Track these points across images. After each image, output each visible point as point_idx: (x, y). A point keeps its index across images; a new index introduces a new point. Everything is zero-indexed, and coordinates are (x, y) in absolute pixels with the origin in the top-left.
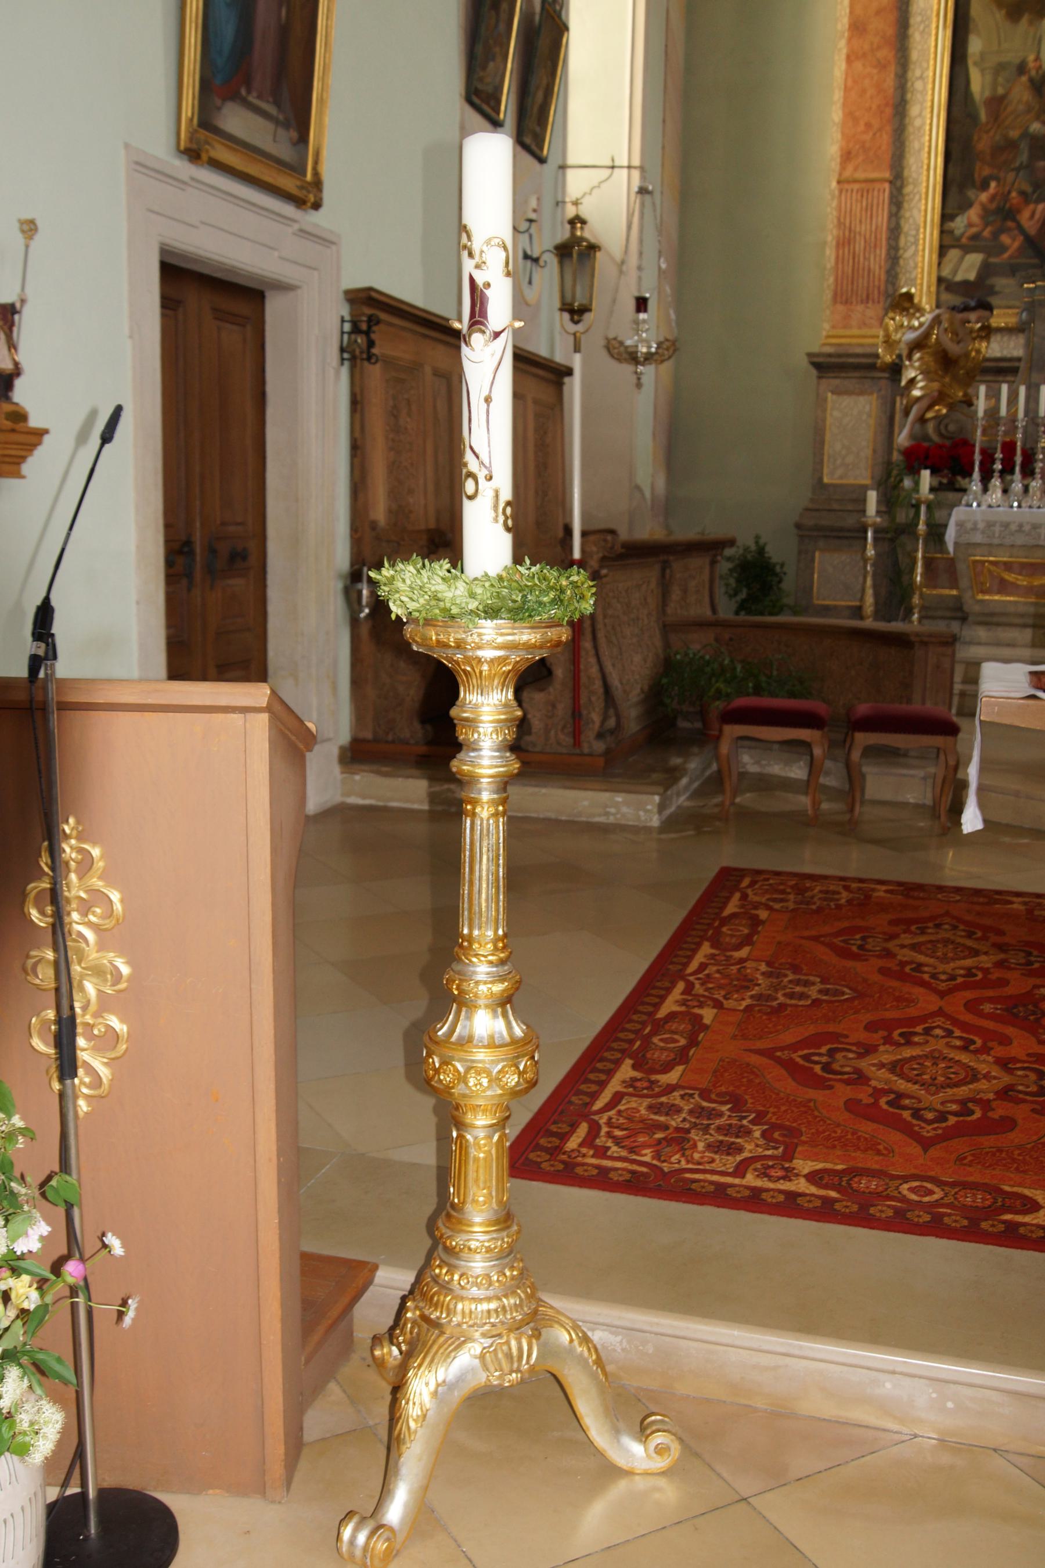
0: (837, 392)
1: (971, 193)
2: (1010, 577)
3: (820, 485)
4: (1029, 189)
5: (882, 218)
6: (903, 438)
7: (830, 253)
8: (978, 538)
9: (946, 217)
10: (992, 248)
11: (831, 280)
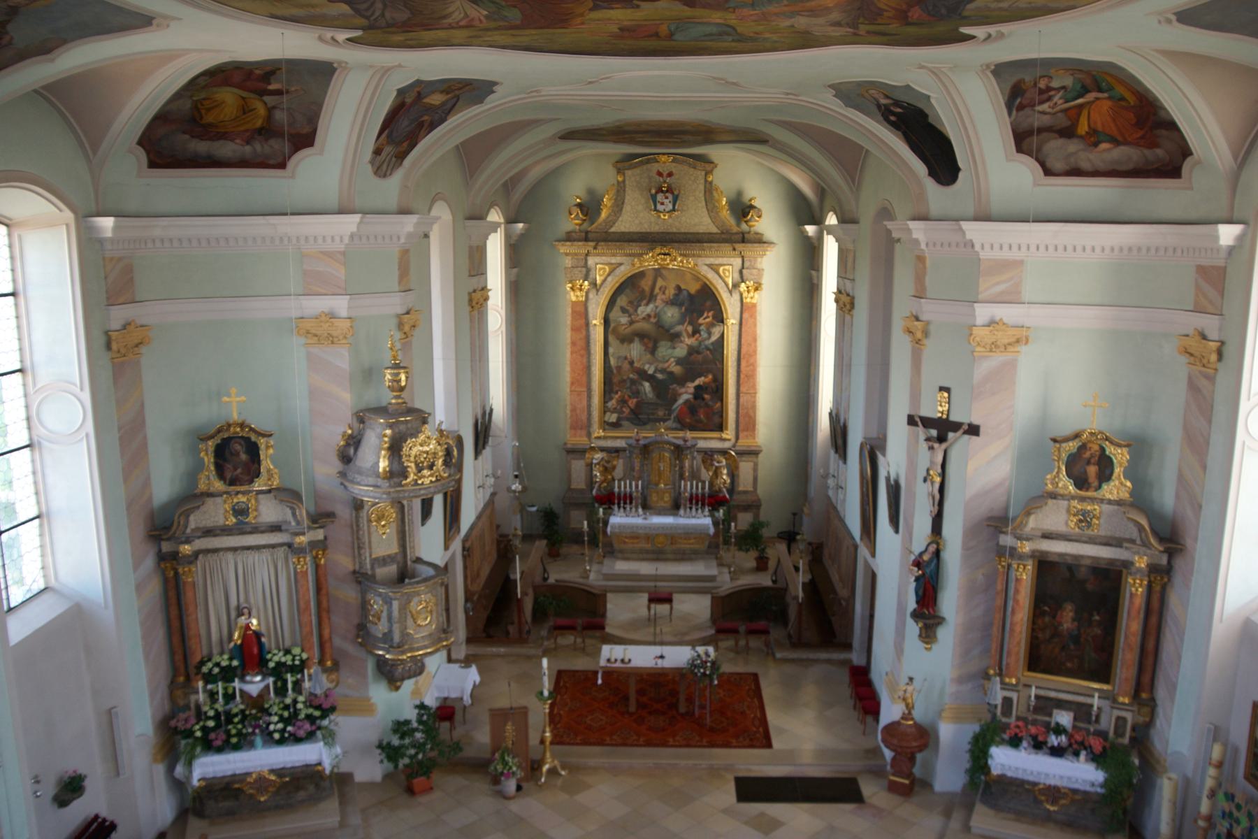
0: (574, 459)
1: (613, 395)
2: (627, 540)
3: (569, 489)
4: (630, 394)
5: (585, 403)
6: (594, 492)
7: (568, 412)
8: (617, 530)
9: (605, 402)
10: (621, 412)
11: (569, 421)
